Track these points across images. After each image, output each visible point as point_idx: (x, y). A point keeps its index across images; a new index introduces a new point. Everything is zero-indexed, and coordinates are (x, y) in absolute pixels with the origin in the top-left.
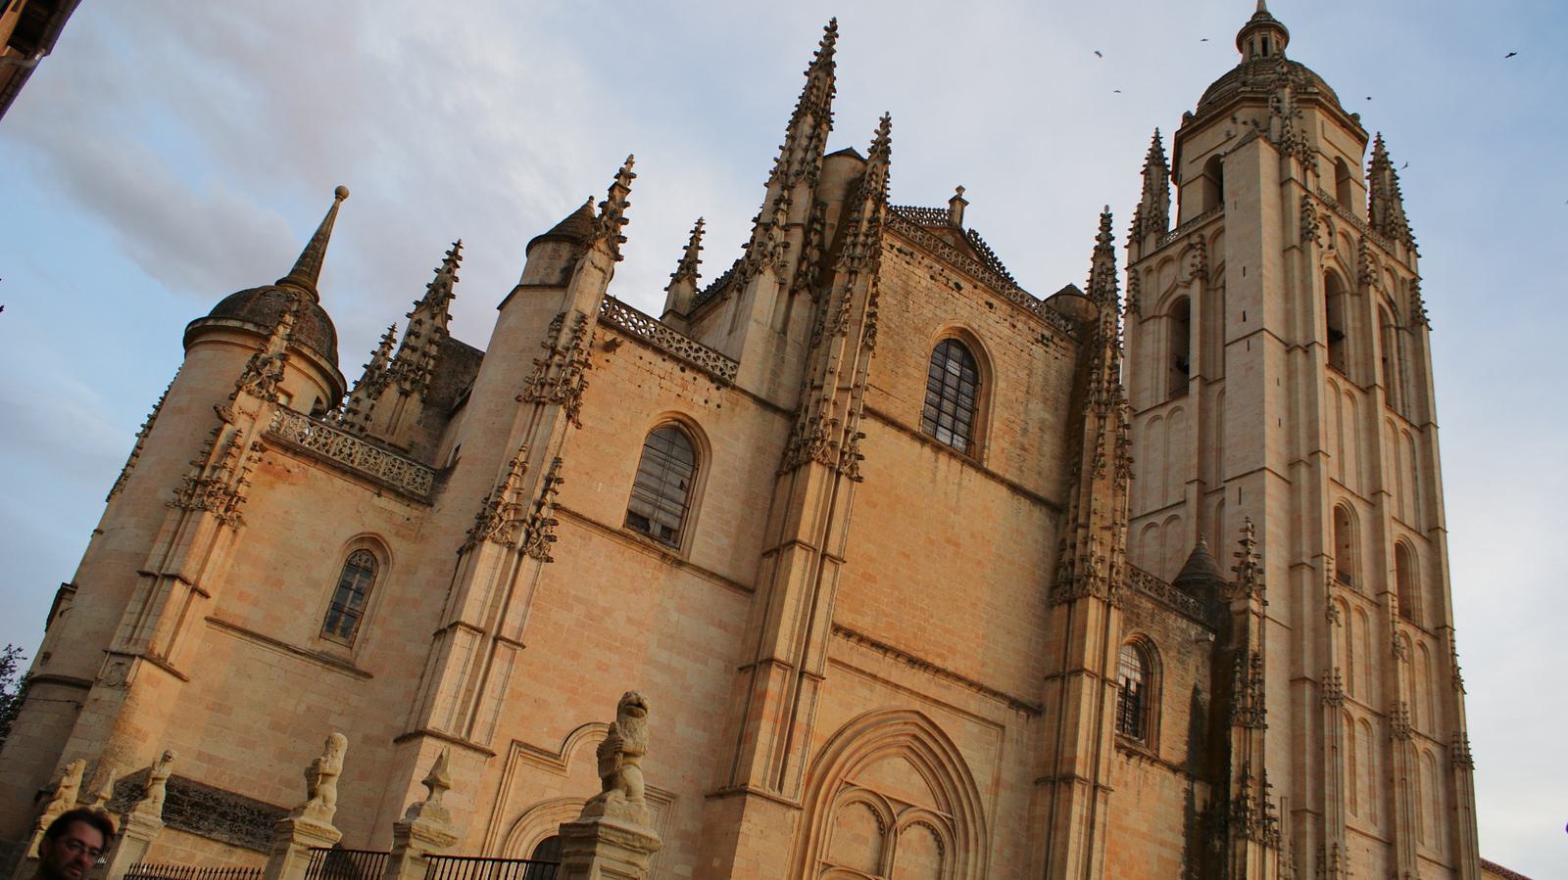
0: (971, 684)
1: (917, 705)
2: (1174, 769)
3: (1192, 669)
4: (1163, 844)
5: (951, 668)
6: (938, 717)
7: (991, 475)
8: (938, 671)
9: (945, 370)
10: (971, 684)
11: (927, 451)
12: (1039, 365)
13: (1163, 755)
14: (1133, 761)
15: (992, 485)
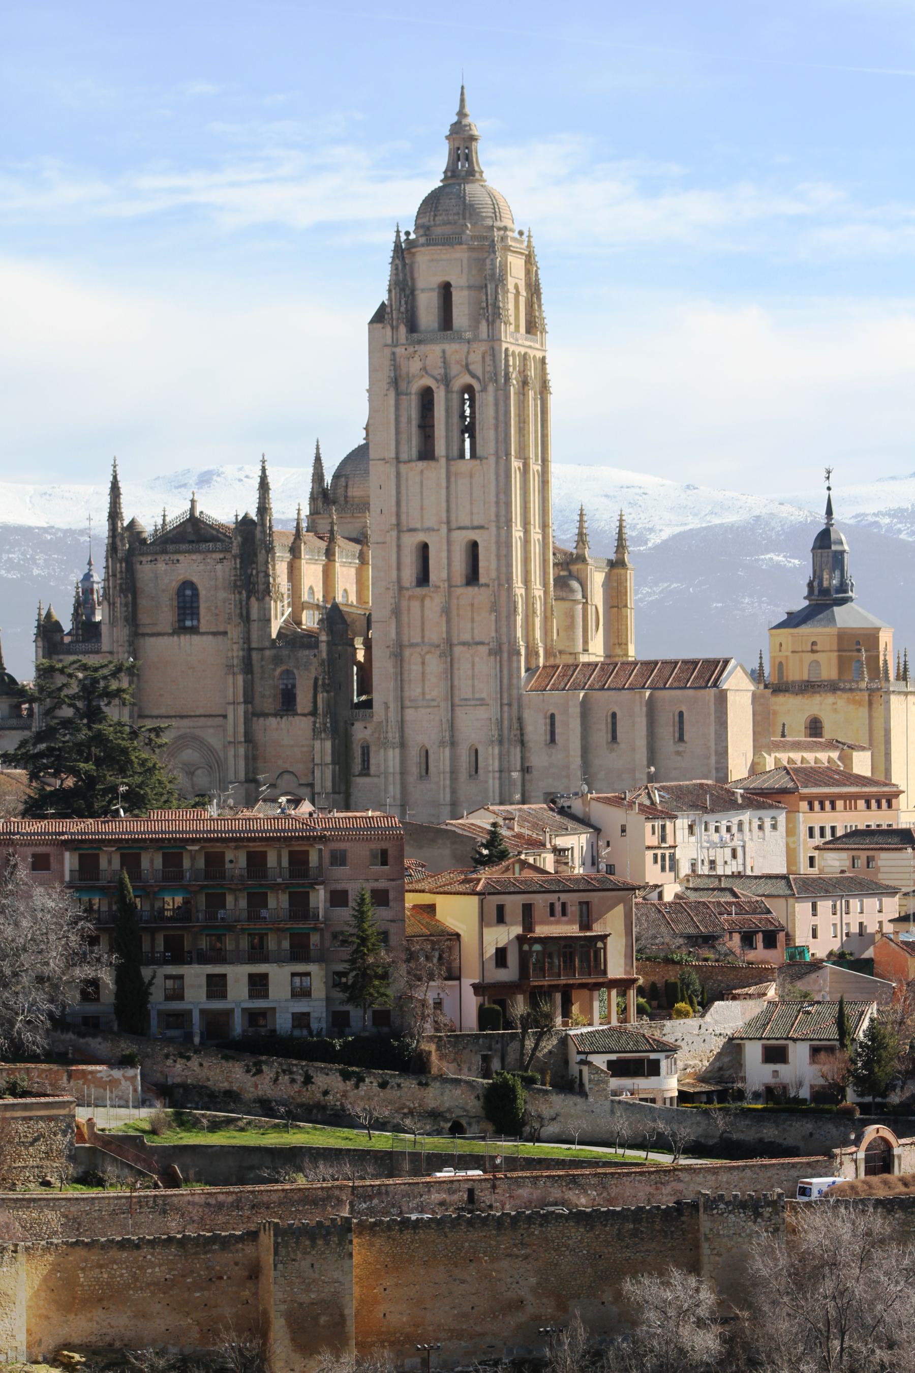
0: (205, 716)
1: (188, 730)
2: (304, 715)
3: (313, 670)
4: (303, 746)
5: (197, 713)
6: (198, 732)
7: (203, 634)
8: (191, 716)
9: (184, 596)
10: (205, 716)
11: (176, 638)
12: (220, 574)
13: (299, 711)
14: (285, 718)
15: (205, 638)
